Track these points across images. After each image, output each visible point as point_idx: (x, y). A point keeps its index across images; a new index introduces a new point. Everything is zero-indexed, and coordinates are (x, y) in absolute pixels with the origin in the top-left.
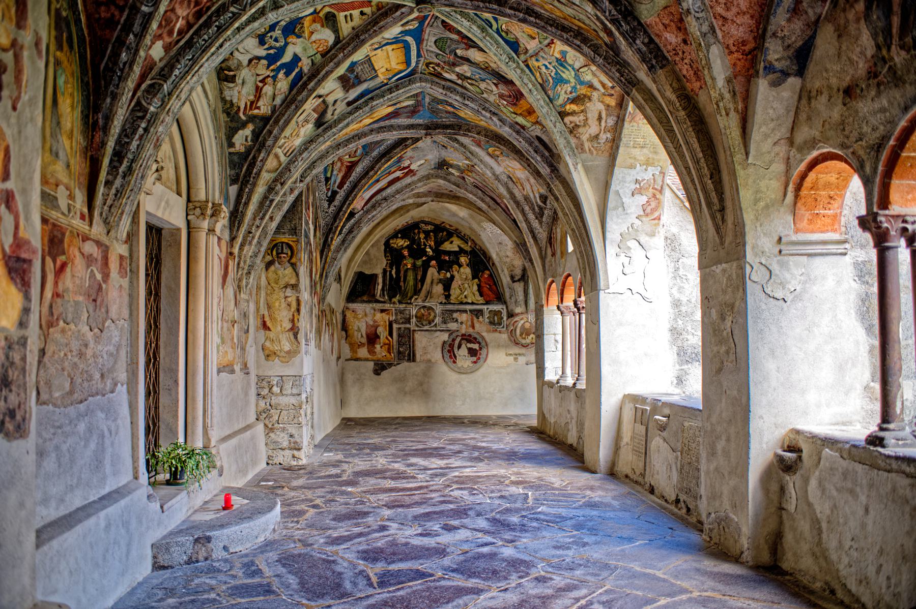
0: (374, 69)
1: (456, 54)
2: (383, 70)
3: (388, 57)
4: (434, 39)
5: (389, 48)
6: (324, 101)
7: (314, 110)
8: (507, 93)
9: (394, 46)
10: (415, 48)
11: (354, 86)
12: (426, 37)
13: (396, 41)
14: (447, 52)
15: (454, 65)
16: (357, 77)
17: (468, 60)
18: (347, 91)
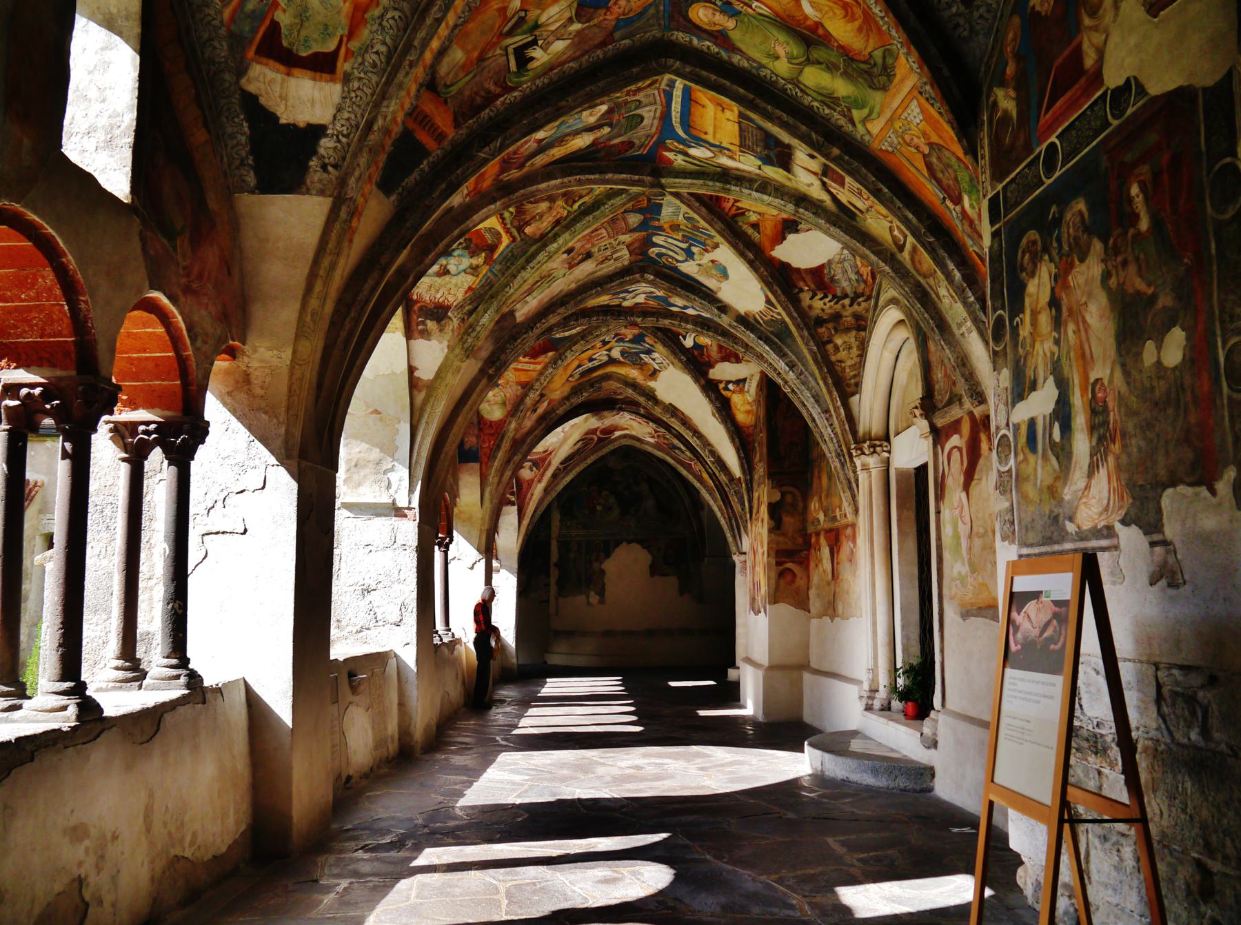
0: (741, 129)
1: (610, 125)
2: (728, 114)
3: (715, 127)
4: (645, 122)
5: (709, 138)
6: (825, 174)
7: (842, 184)
8: (522, 150)
9: (704, 137)
10: (673, 114)
11: (778, 142)
12: (656, 122)
13: (700, 142)
14: (623, 121)
15: (610, 112)
16: (767, 147)
17: (590, 129)
18: (789, 147)
